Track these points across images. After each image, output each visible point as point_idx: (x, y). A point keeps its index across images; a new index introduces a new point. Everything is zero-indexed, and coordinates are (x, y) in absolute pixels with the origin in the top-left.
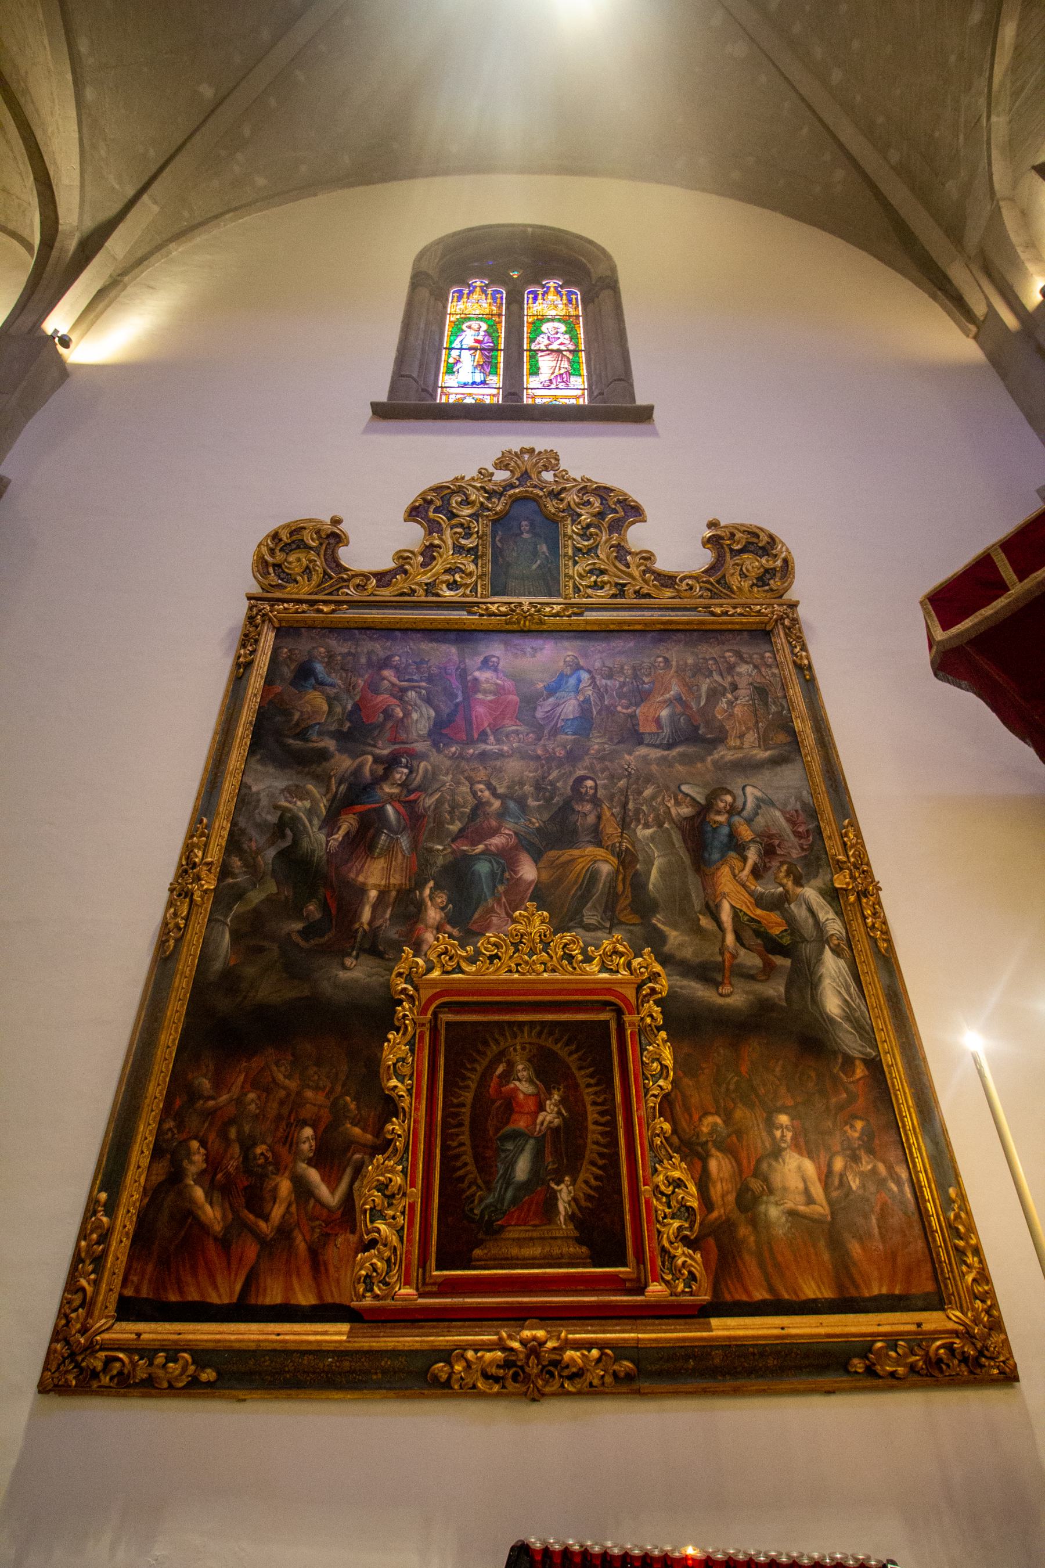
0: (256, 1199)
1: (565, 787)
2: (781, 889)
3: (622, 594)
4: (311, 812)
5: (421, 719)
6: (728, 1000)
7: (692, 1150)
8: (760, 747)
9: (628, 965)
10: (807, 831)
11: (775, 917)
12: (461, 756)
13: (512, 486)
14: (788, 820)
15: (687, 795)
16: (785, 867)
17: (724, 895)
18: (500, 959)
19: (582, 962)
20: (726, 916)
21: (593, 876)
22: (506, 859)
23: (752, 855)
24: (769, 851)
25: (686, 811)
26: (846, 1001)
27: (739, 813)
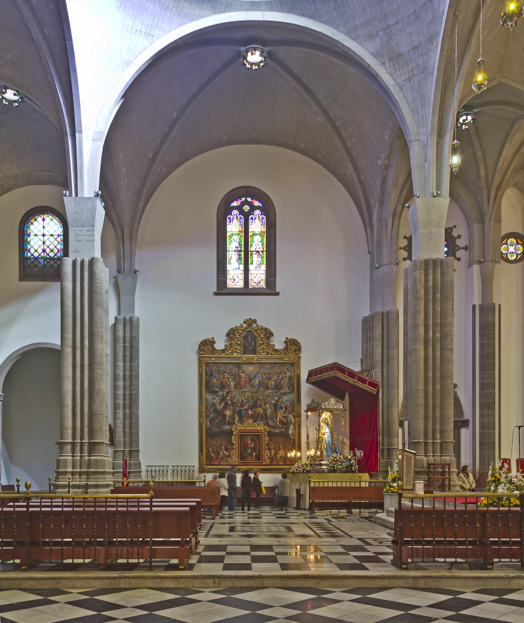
0: (219, 454)
1: (256, 398)
3: (268, 354)
4: (217, 402)
5: (232, 384)
7: (270, 450)
11: (285, 419)
12: (239, 392)
13: (247, 328)
21: (260, 413)
22: (247, 410)
23: (283, 410)
24: (286, 409)
25: (274, 402)
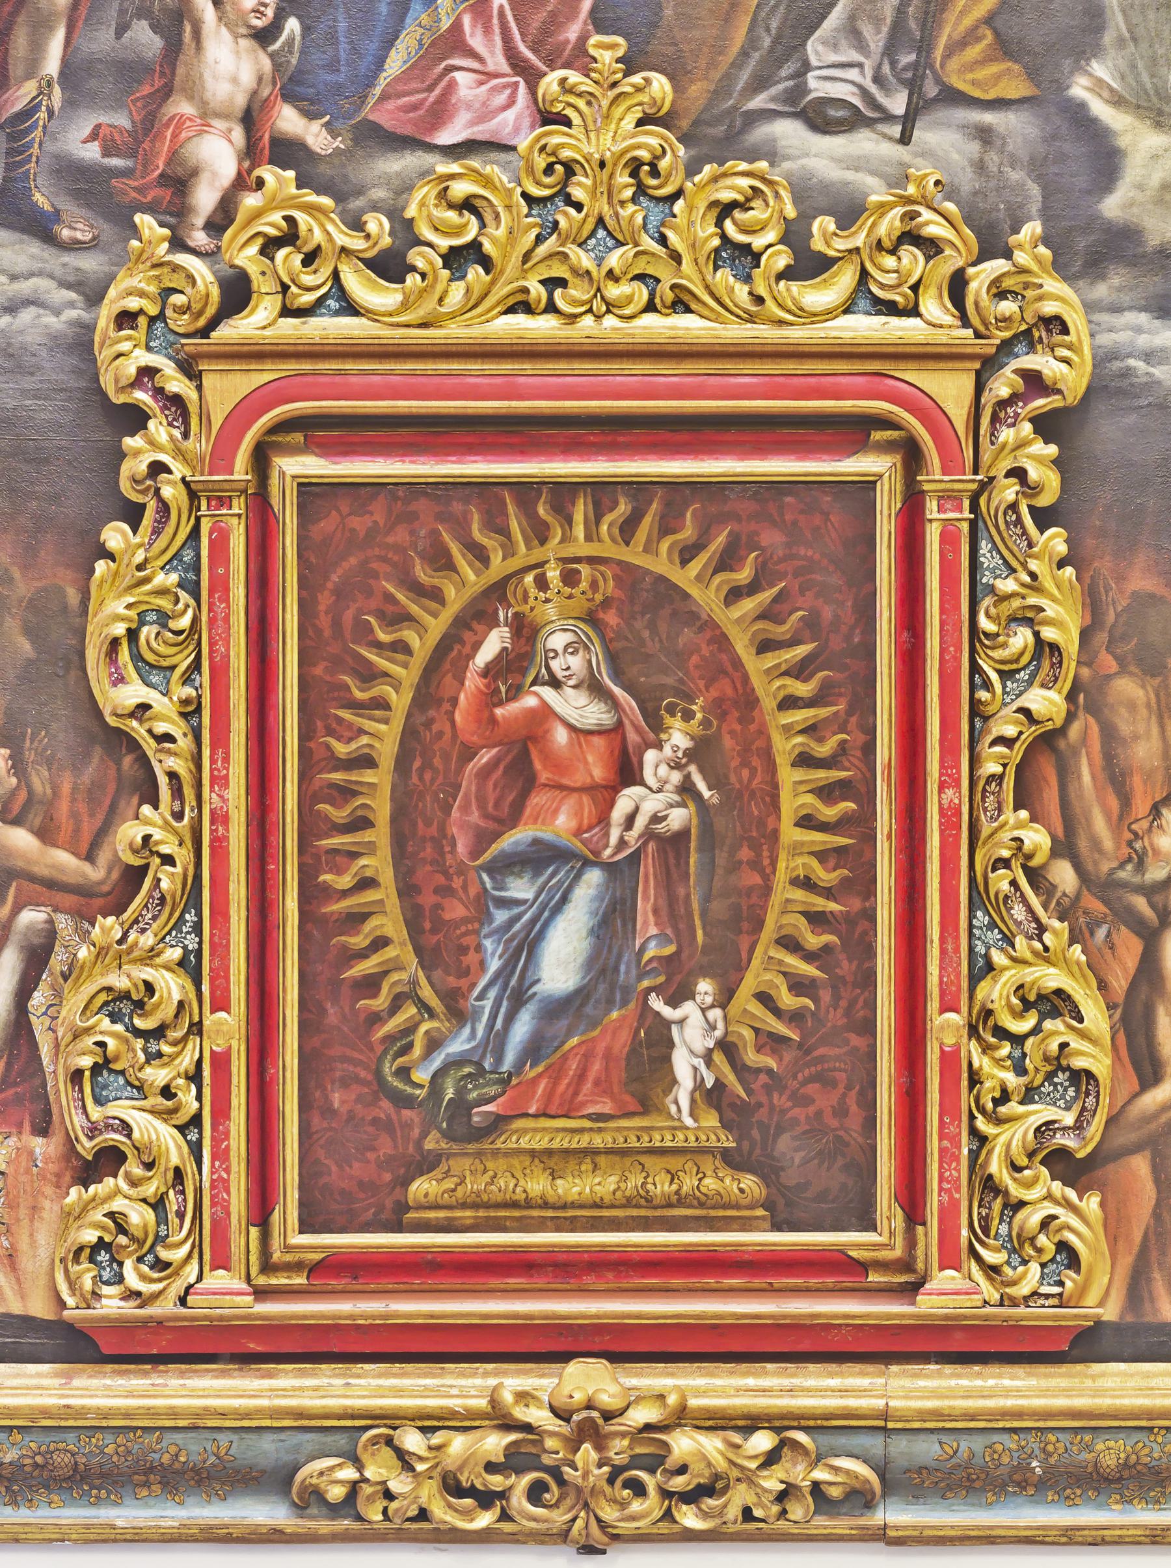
9: (957, 286)
18: (486, 263)
19: (786, 274)
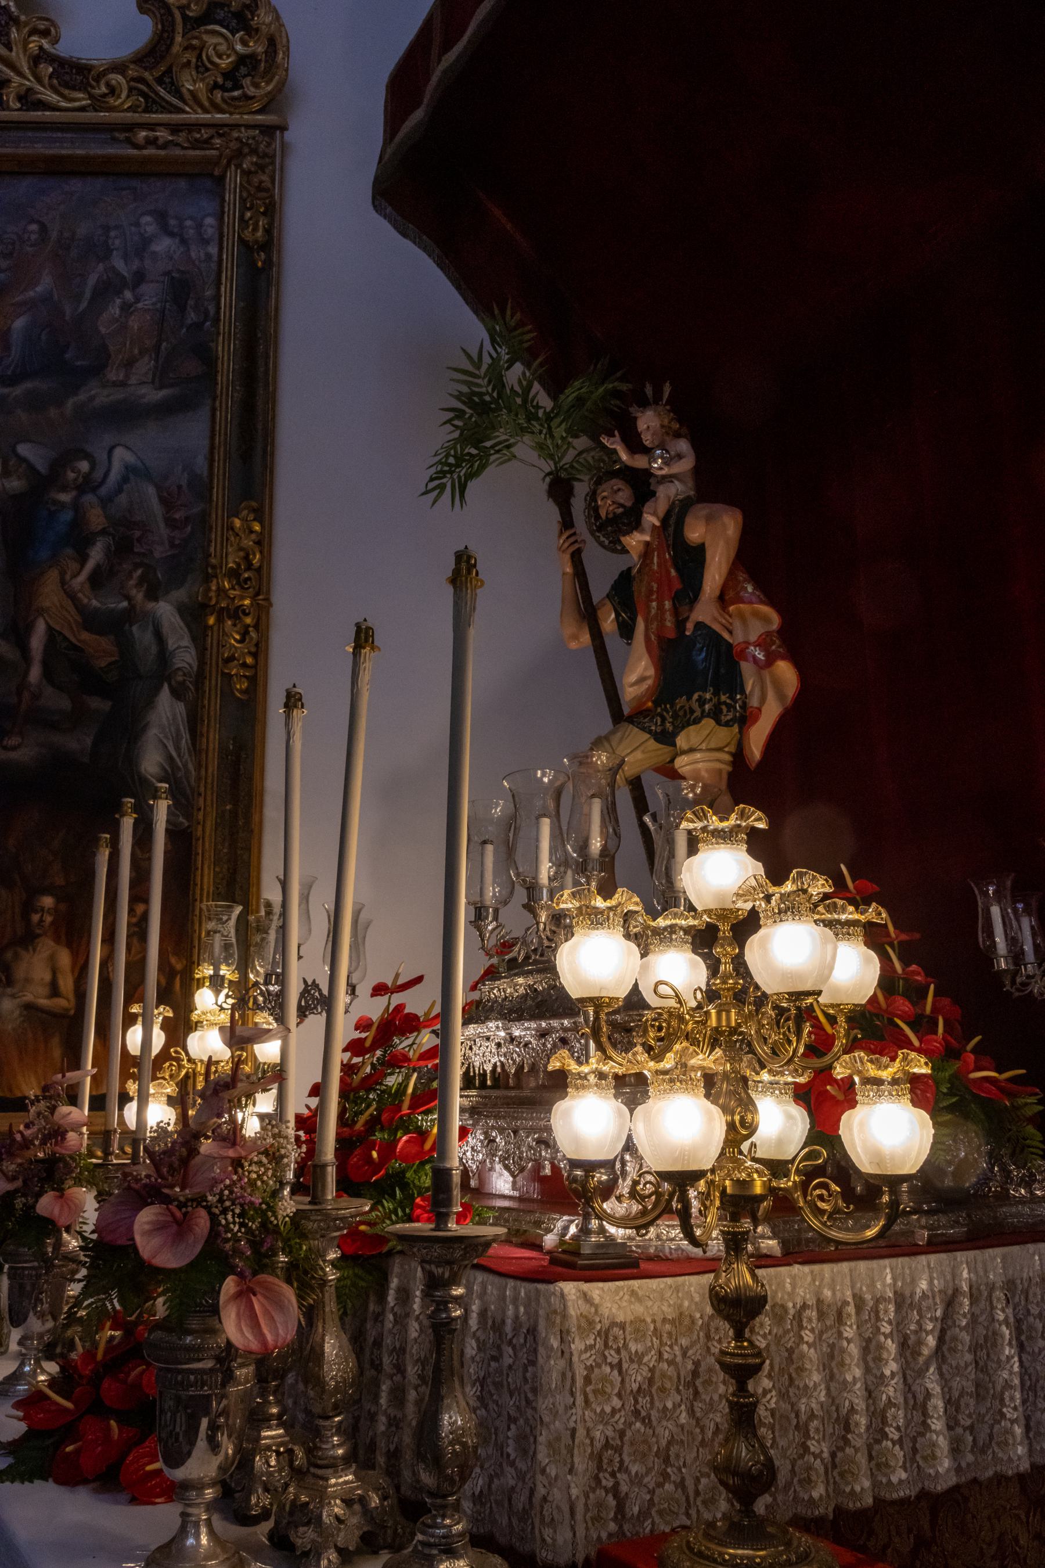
2: (125, 604)
6: (13, 755)
8: (153, 382)
10: (187, 518)
11: (106, 643)
14: (162, 500)
15: (22, 460)
16: (139, 572)
17: (41, 612)
20: (37, 642)
23: (96, 554)
26: (170, 758)
27: (94, 490)
